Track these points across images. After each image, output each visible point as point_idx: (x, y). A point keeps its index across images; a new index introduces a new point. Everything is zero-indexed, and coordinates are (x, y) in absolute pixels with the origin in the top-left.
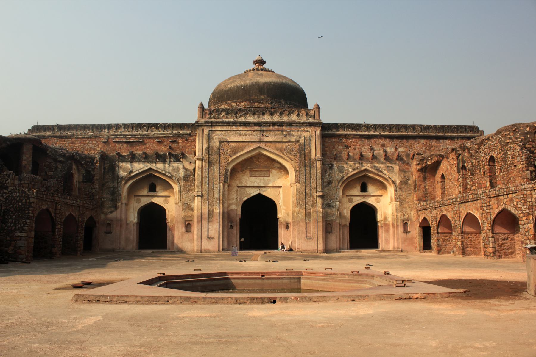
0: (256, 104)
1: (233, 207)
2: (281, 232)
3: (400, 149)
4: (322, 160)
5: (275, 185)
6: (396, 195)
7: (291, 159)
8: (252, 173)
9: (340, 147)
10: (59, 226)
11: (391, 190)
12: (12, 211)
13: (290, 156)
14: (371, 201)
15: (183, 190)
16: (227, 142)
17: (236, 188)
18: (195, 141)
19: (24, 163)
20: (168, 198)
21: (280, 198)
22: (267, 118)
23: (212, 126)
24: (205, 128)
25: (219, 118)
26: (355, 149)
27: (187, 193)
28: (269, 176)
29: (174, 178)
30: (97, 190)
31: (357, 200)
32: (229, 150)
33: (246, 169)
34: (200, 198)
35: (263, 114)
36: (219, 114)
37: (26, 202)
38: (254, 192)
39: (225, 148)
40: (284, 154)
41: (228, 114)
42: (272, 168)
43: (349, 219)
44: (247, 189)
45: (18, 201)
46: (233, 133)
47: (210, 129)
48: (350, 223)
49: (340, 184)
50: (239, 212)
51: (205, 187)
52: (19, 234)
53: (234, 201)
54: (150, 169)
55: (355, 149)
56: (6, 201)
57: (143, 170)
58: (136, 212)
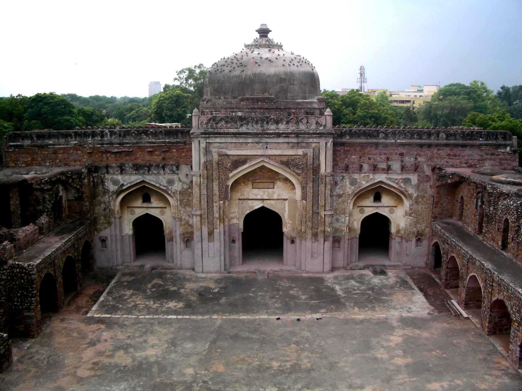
0: (260, 103)
1: (235, 221)
2: (287, 245)
3: (420, 159)
4: (332, 176)
6: (411, 209)
7: (298, 174)
8: (254, 185)
9: (353, 157)
10: (60, 279)
11: (407, 203)
12: (16, 289)
13: (296, 171)
14: (385, 212)
17: (237, 202)
18: (191, 150)
19: (12, 208)
20: (165, 209)
21: (286, 211)
22: (272, 128)
24: (202, 140)
25: (217, 128)
26: (369, 159)
28: (274, 188)
29: (170, 192)
30: (88, 208)
31: (369, 212)
32: (229, 165)
33: (248, 180)
35: (267, 123)
36: (217, 123)
37: (28, 279)
38: (257, 205)
39: (224, 162)
40: (290, 169)
41: (227, 122)
42: (277, 179)
43: (359, 231)
44: (250, 202)
45: (19, 278)
46: (233, 145)
48: (360, 236)
49: (351, 198)
50: (241, 226)
51: (204, 205)
52: (28, 314)
53: (235, 214)
54: (143, 181)
55: (369, 159)
56: (8, 277)
57: (135, 183)
58: (131, 224)
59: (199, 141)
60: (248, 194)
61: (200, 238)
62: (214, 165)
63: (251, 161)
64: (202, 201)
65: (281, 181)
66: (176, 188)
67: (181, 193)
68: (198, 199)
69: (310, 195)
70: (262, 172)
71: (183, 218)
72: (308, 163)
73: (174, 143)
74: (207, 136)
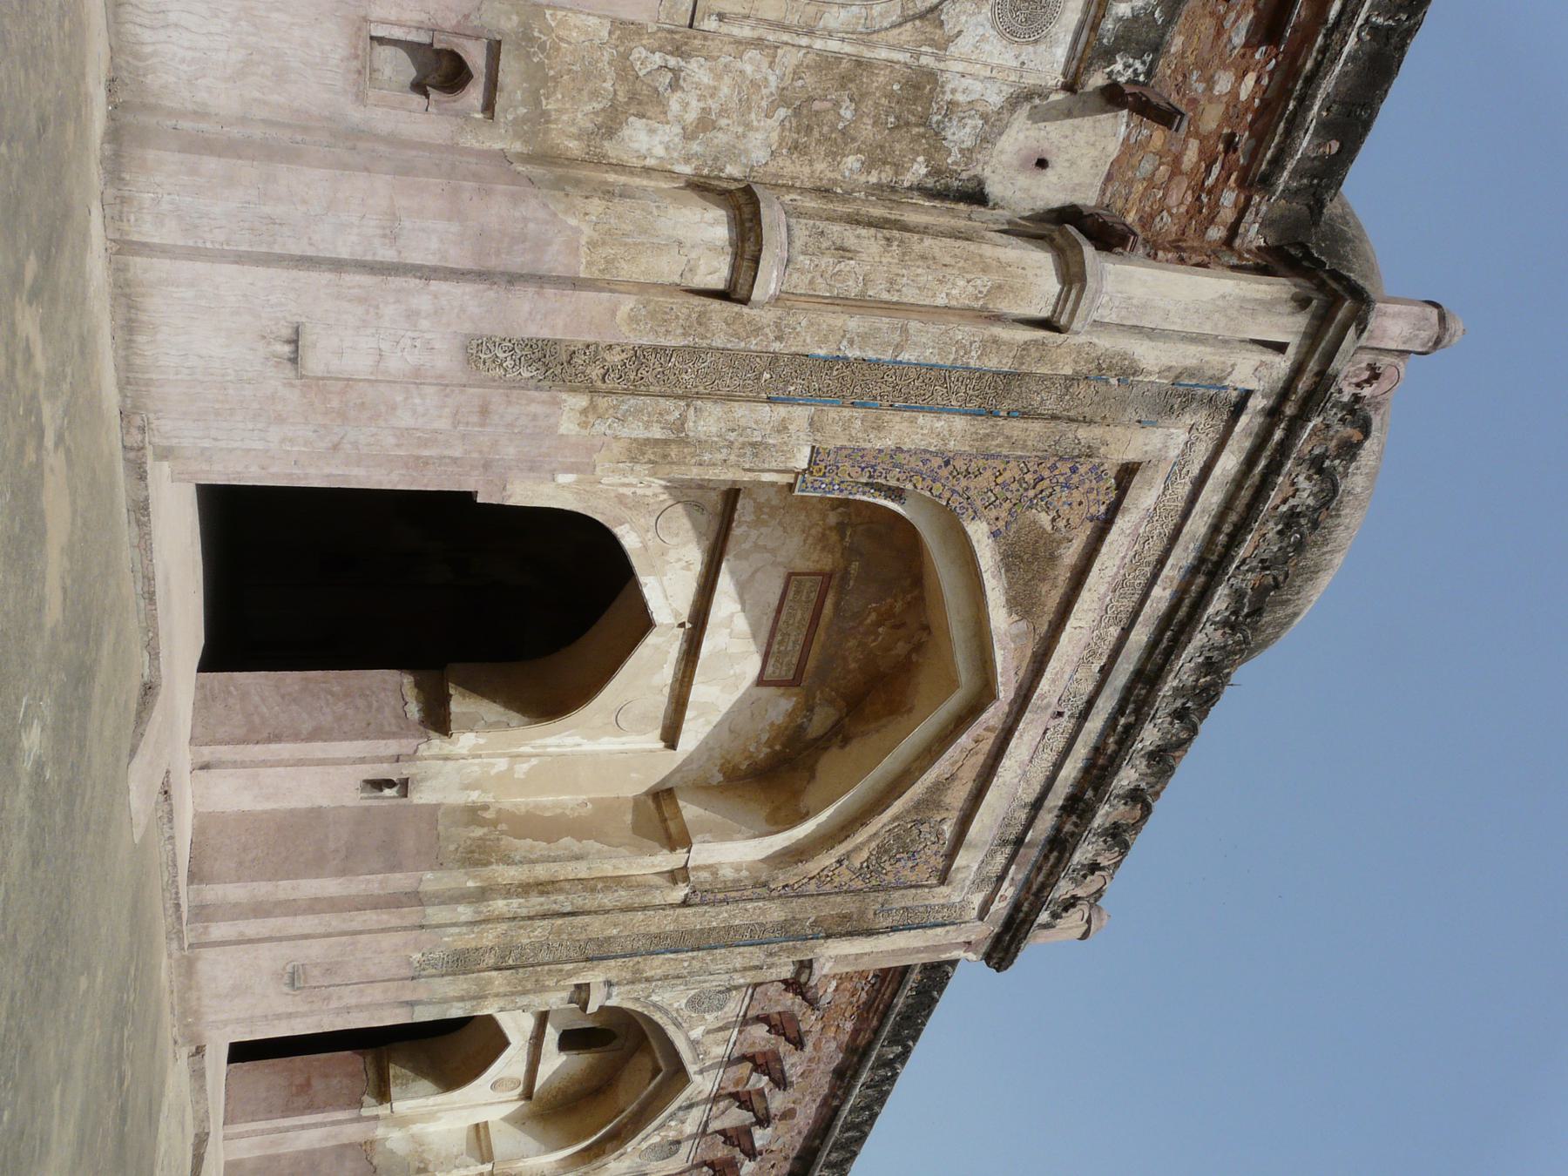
5: (689, 714)
7: (848, 855)
15: (827, 62)
16: (1114, 509)
21: (590, 738)
23: (1273, 414)
24: (1281, 365)
27: (782, 98)
32: (1045, 519)
33: (850, 552)
34: (716, 273)
36: (1317, 465)
38: (666, 588)
39: (1077, 495)
40: (895, 818)
47: (1257, 403)
51: (816, 335)
59: (1280, 348)
60: (757, 547)
61: (517, 261)
62: (1083, 433)
63: (1015, 638)
64: (854, 323)
65: (791, 715)
66: (962, 46)
67: (921, 86)
68: (879, 291)
69: (716, 917)
70: (879, 624)
71: (698, 71)
72: (897, 894)
73: (1304, 102)
74: (1289, 410)
